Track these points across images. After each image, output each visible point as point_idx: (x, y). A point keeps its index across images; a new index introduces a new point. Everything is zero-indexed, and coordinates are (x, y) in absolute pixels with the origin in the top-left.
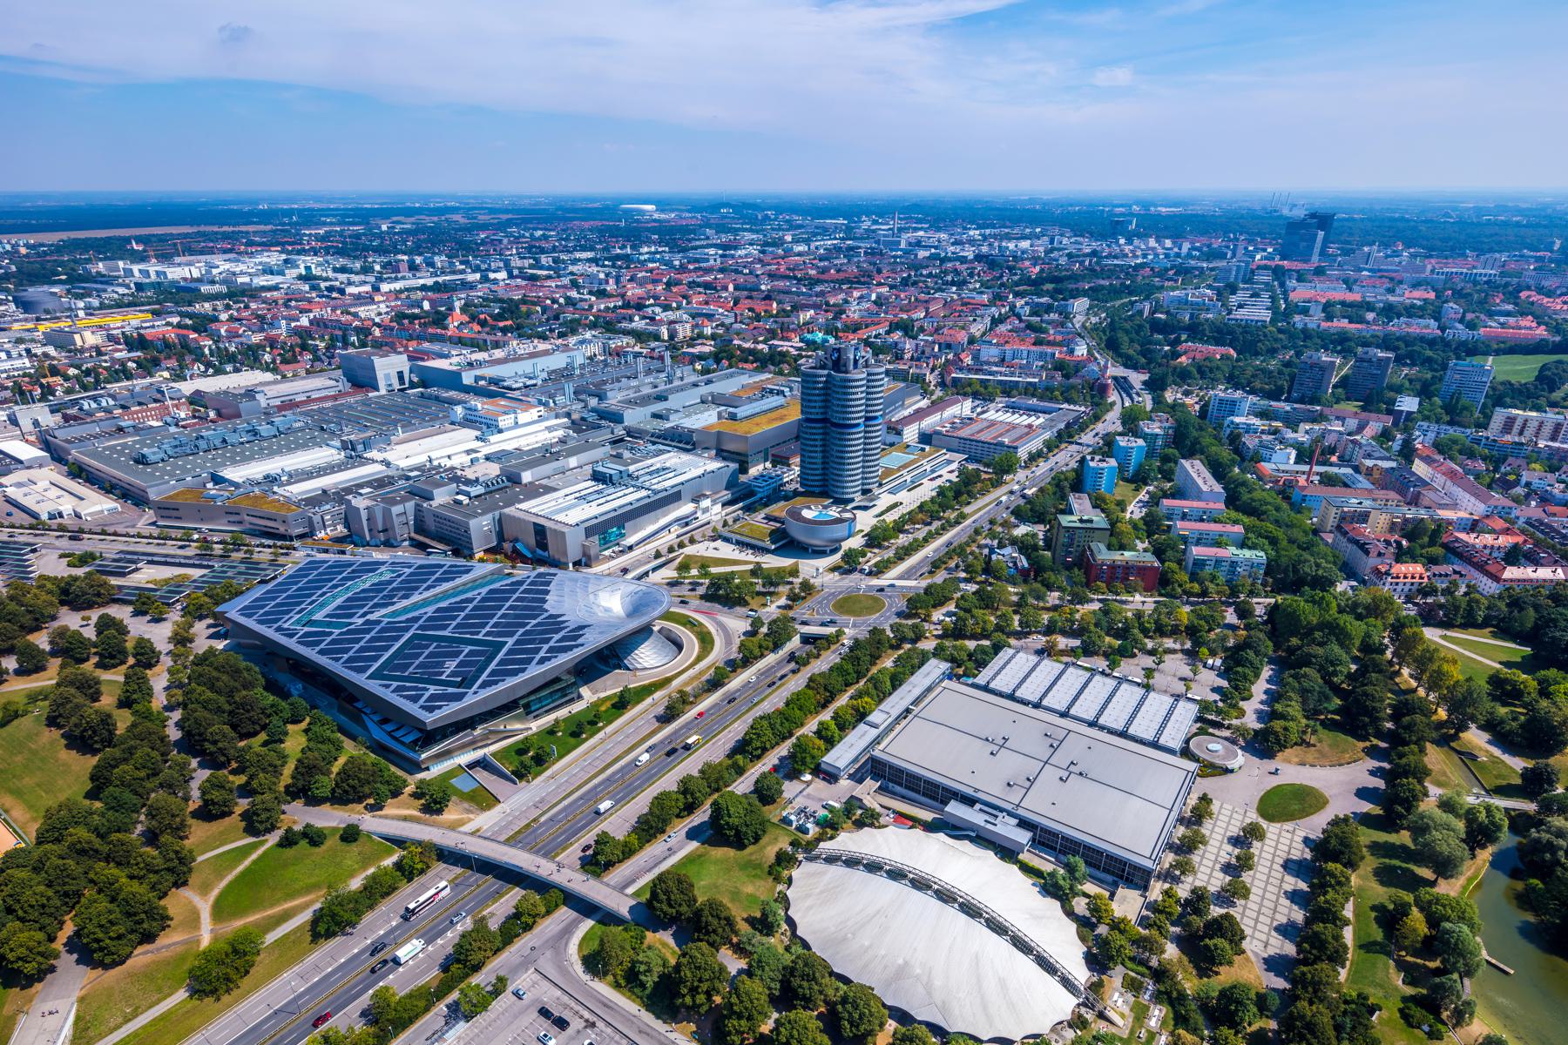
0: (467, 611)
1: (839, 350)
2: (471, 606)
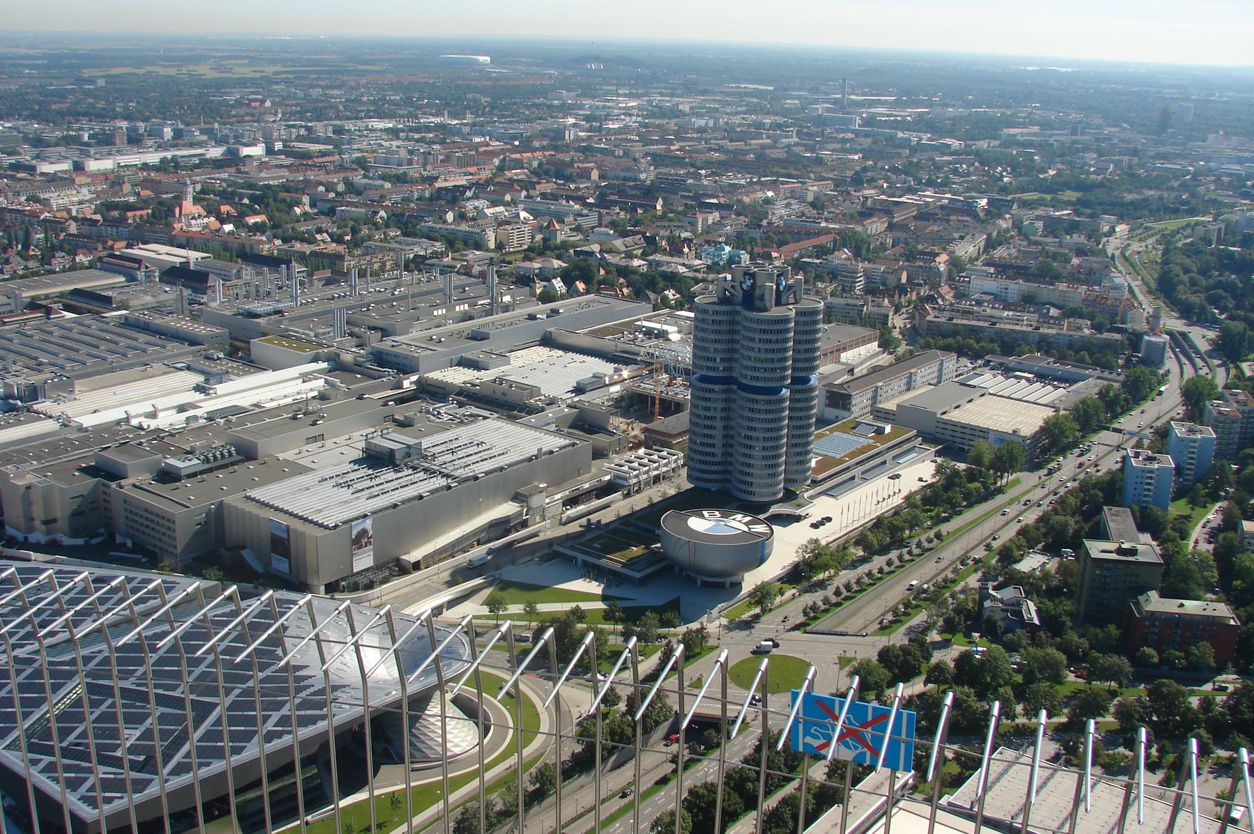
1: (752, 276)
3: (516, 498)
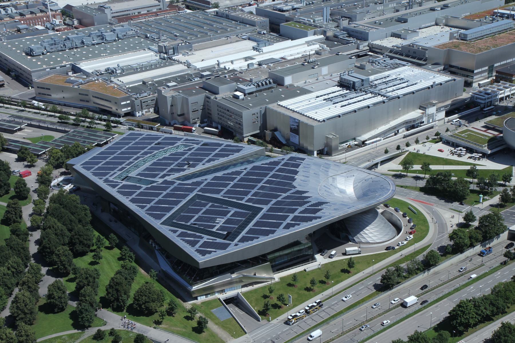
0: (236, 181)
2: (239, 177)
3: (421, 108)
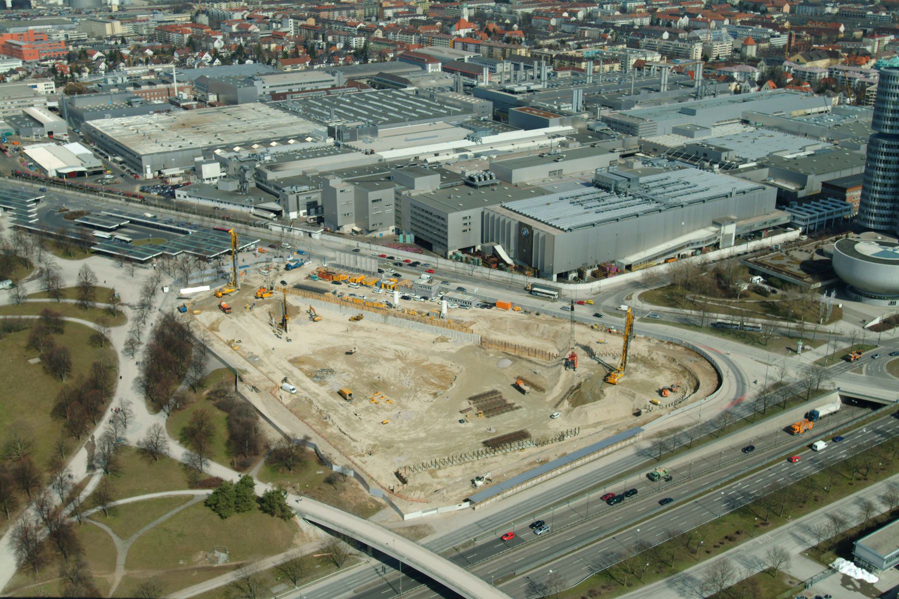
3: (715, 223)
